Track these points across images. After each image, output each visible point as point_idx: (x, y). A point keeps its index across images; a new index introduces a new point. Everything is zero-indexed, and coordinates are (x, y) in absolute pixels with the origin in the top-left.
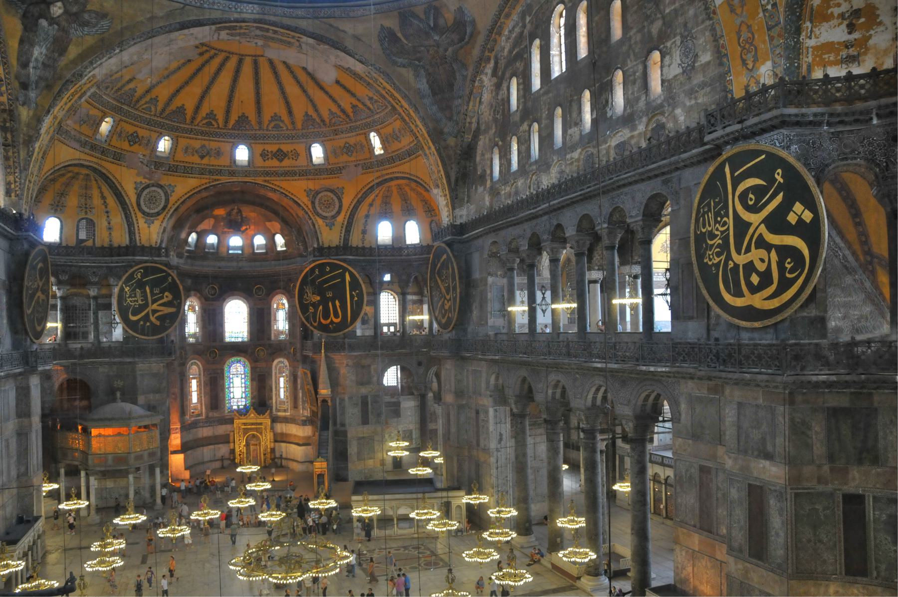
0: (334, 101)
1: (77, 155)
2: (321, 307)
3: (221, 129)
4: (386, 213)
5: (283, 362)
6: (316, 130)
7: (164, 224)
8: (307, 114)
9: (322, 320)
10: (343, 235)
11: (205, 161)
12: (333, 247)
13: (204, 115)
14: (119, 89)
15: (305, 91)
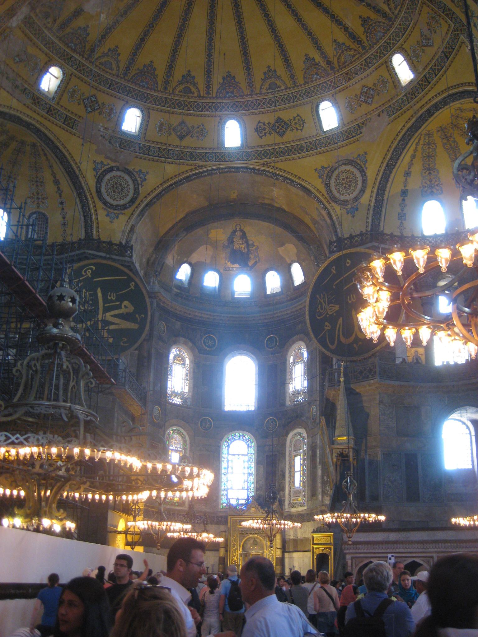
0: (339, 22)
1: (15, 103)
2: (340, 321)
3: (203, 97)
4: (431, 186)
5: (300, 434)
6: (323, 80)
7: (132, 222)
8: (308, 59)
9: (343, 339)
10: (370, 220)
11: (185, 142)
12: (356, 236)
13: (181, 78)
14: (64, 25)
15: (299, 19)
